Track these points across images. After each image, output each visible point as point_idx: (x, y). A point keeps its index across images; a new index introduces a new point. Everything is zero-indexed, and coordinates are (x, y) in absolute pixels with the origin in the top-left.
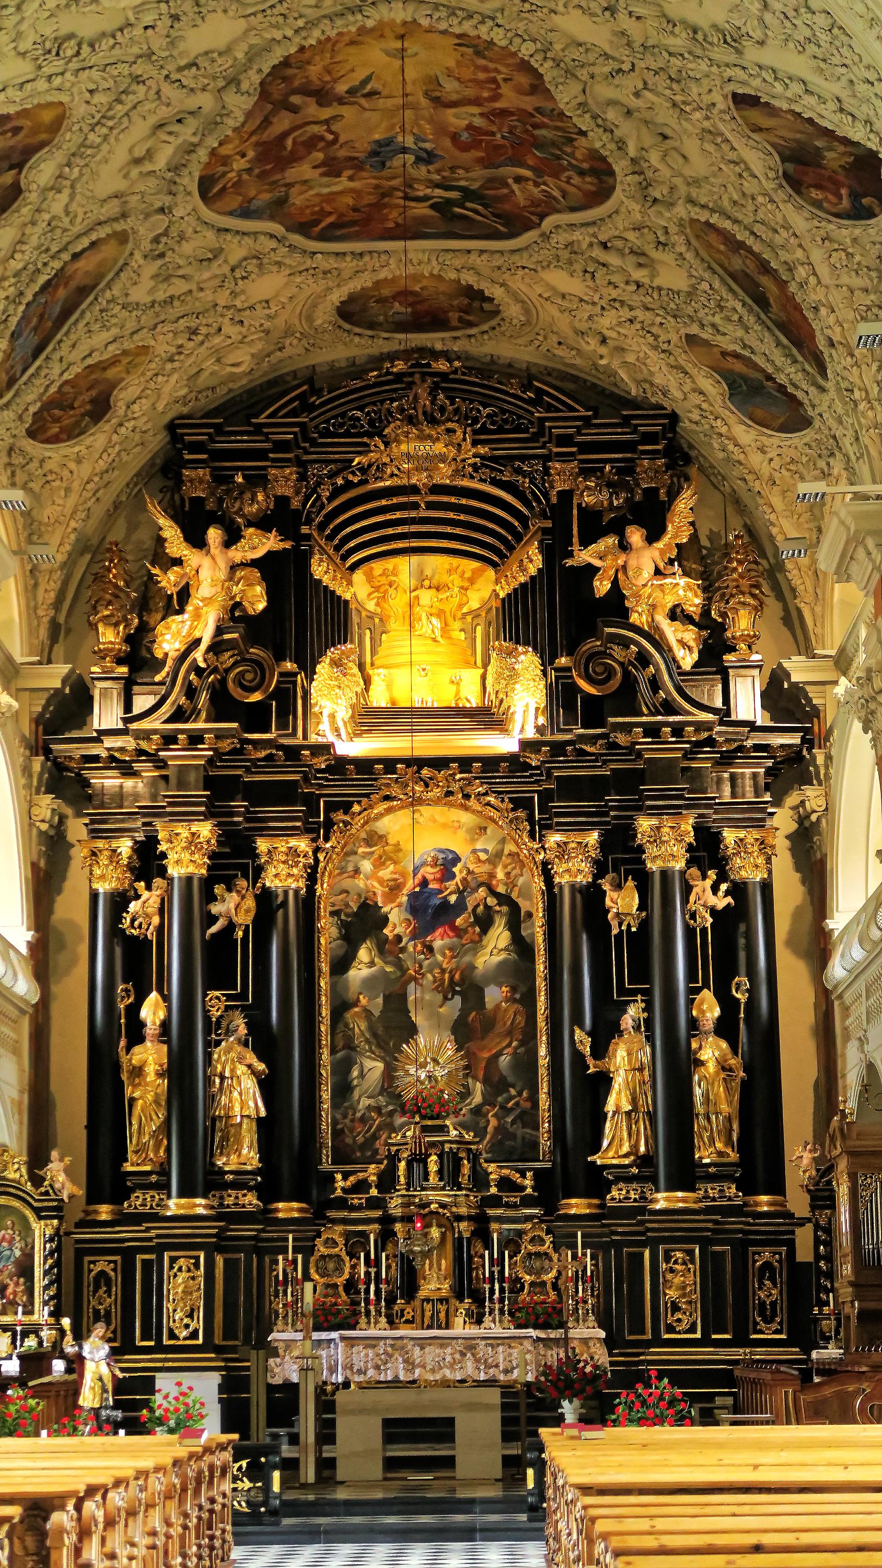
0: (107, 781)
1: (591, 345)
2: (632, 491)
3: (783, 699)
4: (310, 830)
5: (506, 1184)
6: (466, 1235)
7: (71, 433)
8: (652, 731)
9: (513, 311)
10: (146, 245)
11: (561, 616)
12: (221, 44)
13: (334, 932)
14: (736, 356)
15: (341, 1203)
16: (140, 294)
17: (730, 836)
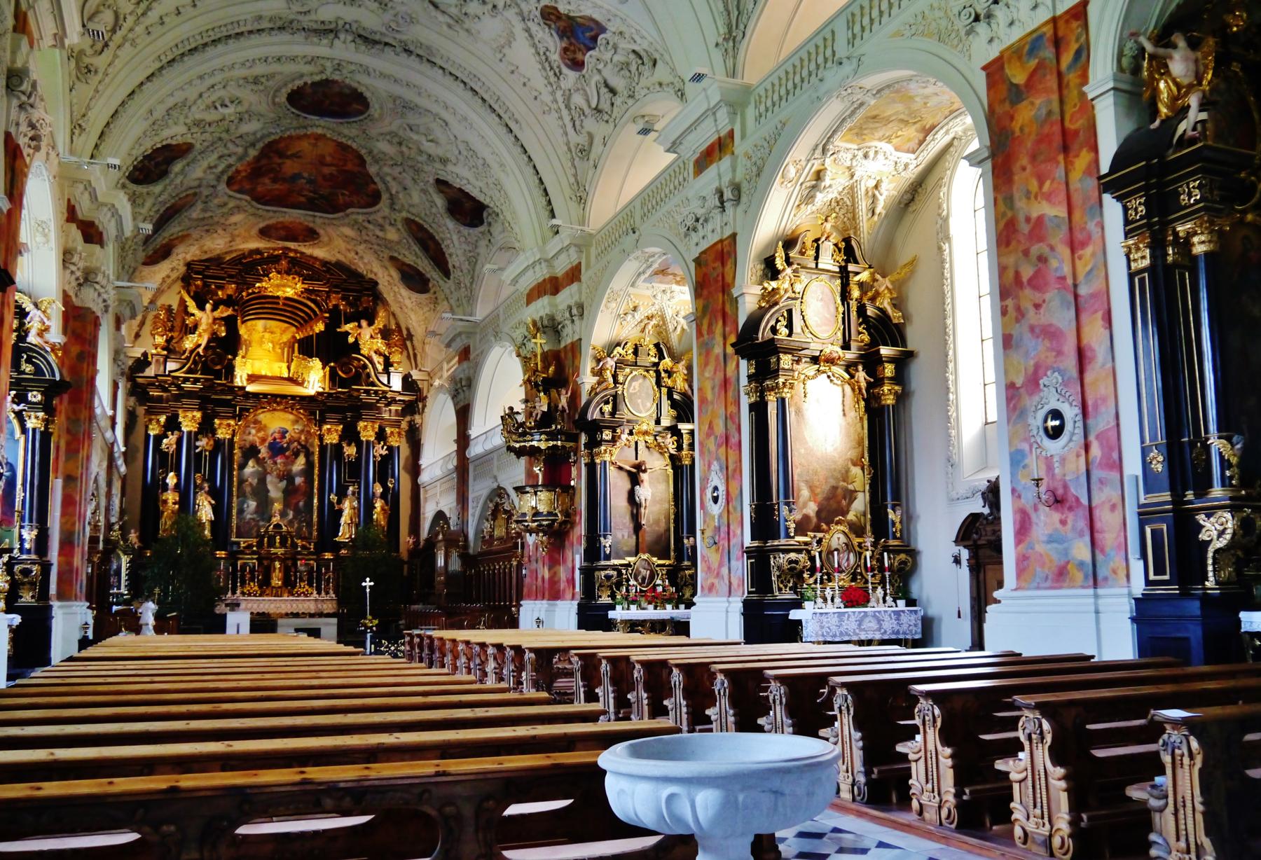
1: (352, 255)
3: (408, 383)
9: (325, 239)
15: (242, 552)
16: (194, 215)
17: (388, 430)
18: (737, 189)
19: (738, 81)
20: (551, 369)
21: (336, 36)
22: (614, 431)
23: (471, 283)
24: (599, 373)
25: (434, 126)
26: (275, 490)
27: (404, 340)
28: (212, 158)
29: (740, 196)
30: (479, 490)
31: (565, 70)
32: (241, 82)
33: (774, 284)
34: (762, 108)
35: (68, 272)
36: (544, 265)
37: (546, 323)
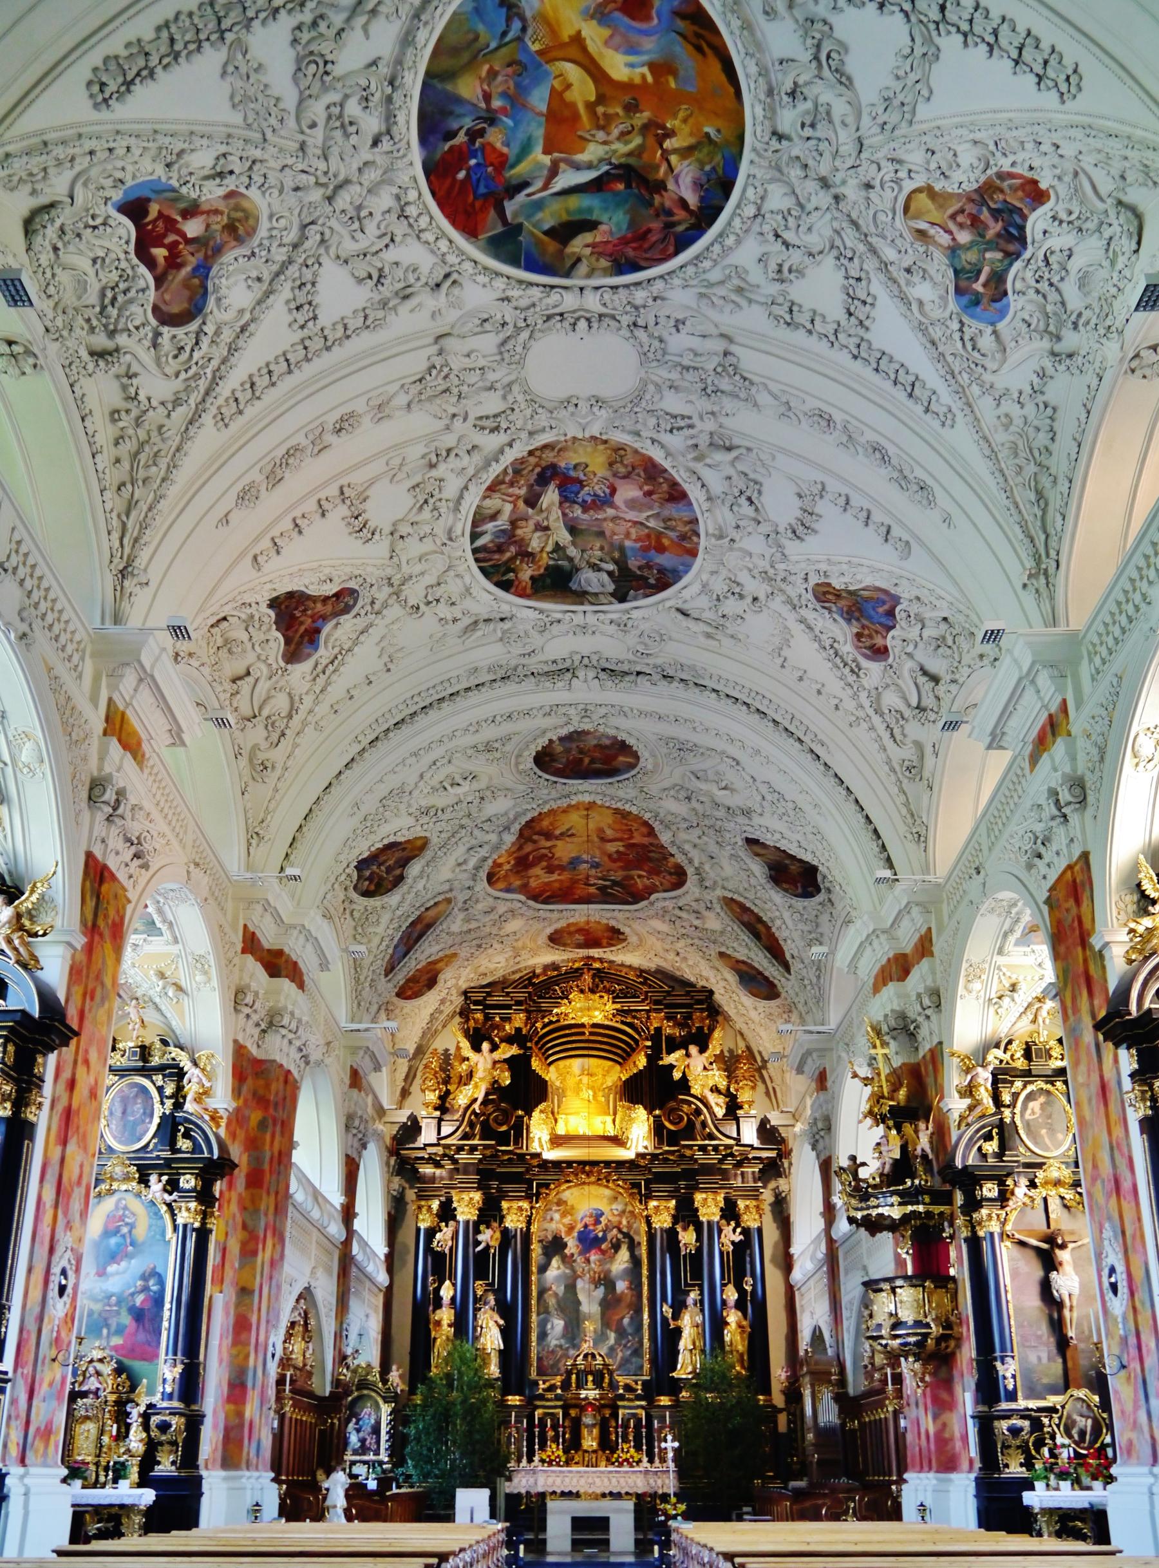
0: (427, 1170)
1: (671, 956)
2: (689, 1027)
3: (767, 1132)
4: (528, 1197)
5: (628, 1388)
7: (417, 995)
8: (703, 1148)
9: (633, 939)
10: (460, 905)
11: (655, 1089)
12: (502, 811)
13: (540, 1251)
14: (743, 962)
15: (542, 1397)
17: (741, 1204)
18: (1078, 785)
19: (1061, 628)
20: (902, 1093)
21: (574, 676)
22: (1002, 1183)
23: (819, 977)
24: (969, 1091)
25: (722, 768)
26: (590, 1302)
27: (759, 1070)
28: (459, 852)
29: (1085, 795)
30: (851, 1289)
31: (865, 663)
32: (470, 752)
33: (1147, 922)
34: (1097, 660)
35: (242, 1016)
36: (883, 937)
37: (893, 1023)
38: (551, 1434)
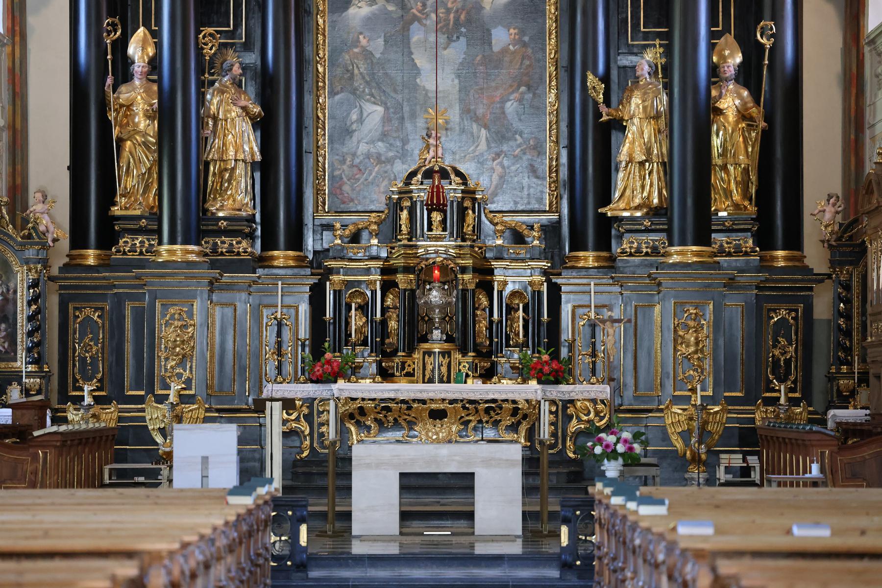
6: (471, 287)
38: (356, 321)
